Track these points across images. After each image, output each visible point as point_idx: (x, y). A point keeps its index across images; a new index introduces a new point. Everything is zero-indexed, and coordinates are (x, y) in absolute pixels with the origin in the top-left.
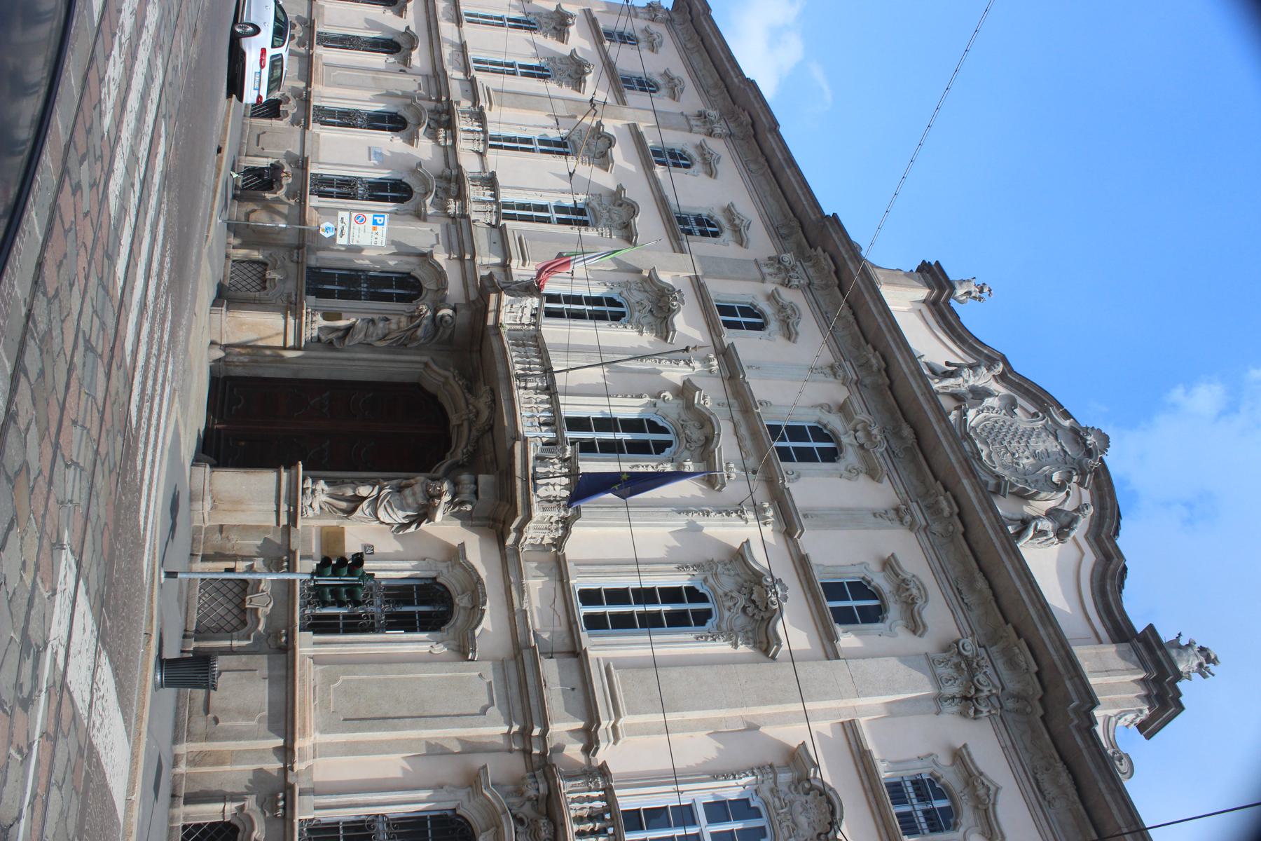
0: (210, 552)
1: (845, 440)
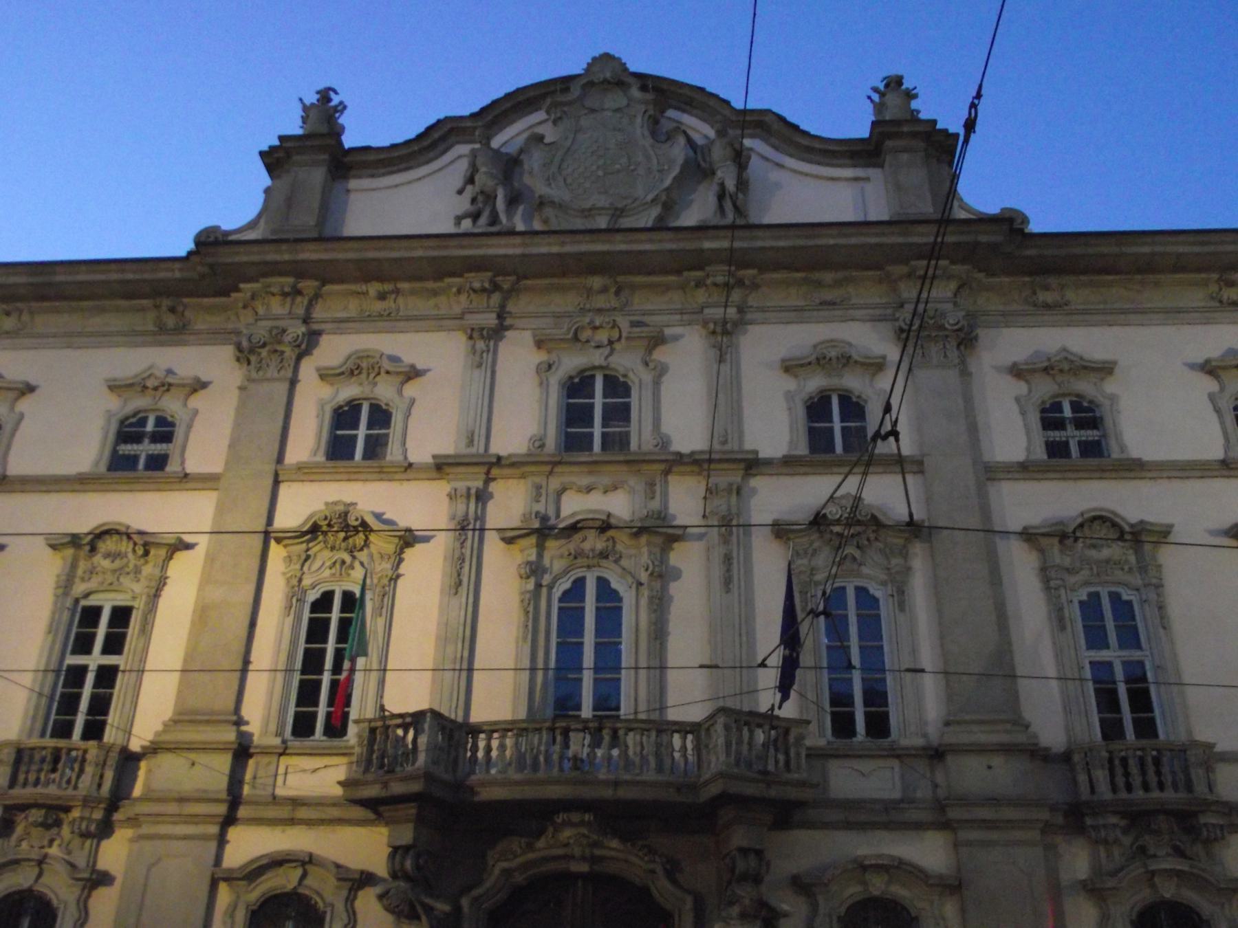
1: (597, 358)
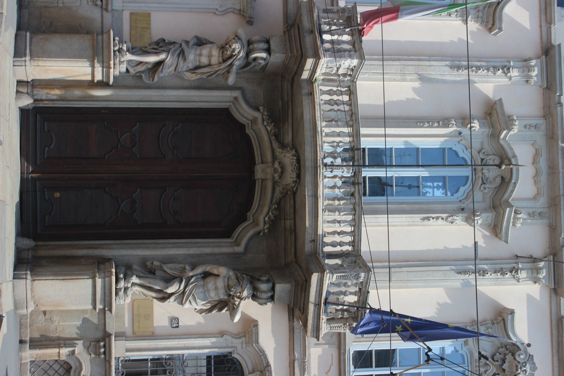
0: (36, 335)
